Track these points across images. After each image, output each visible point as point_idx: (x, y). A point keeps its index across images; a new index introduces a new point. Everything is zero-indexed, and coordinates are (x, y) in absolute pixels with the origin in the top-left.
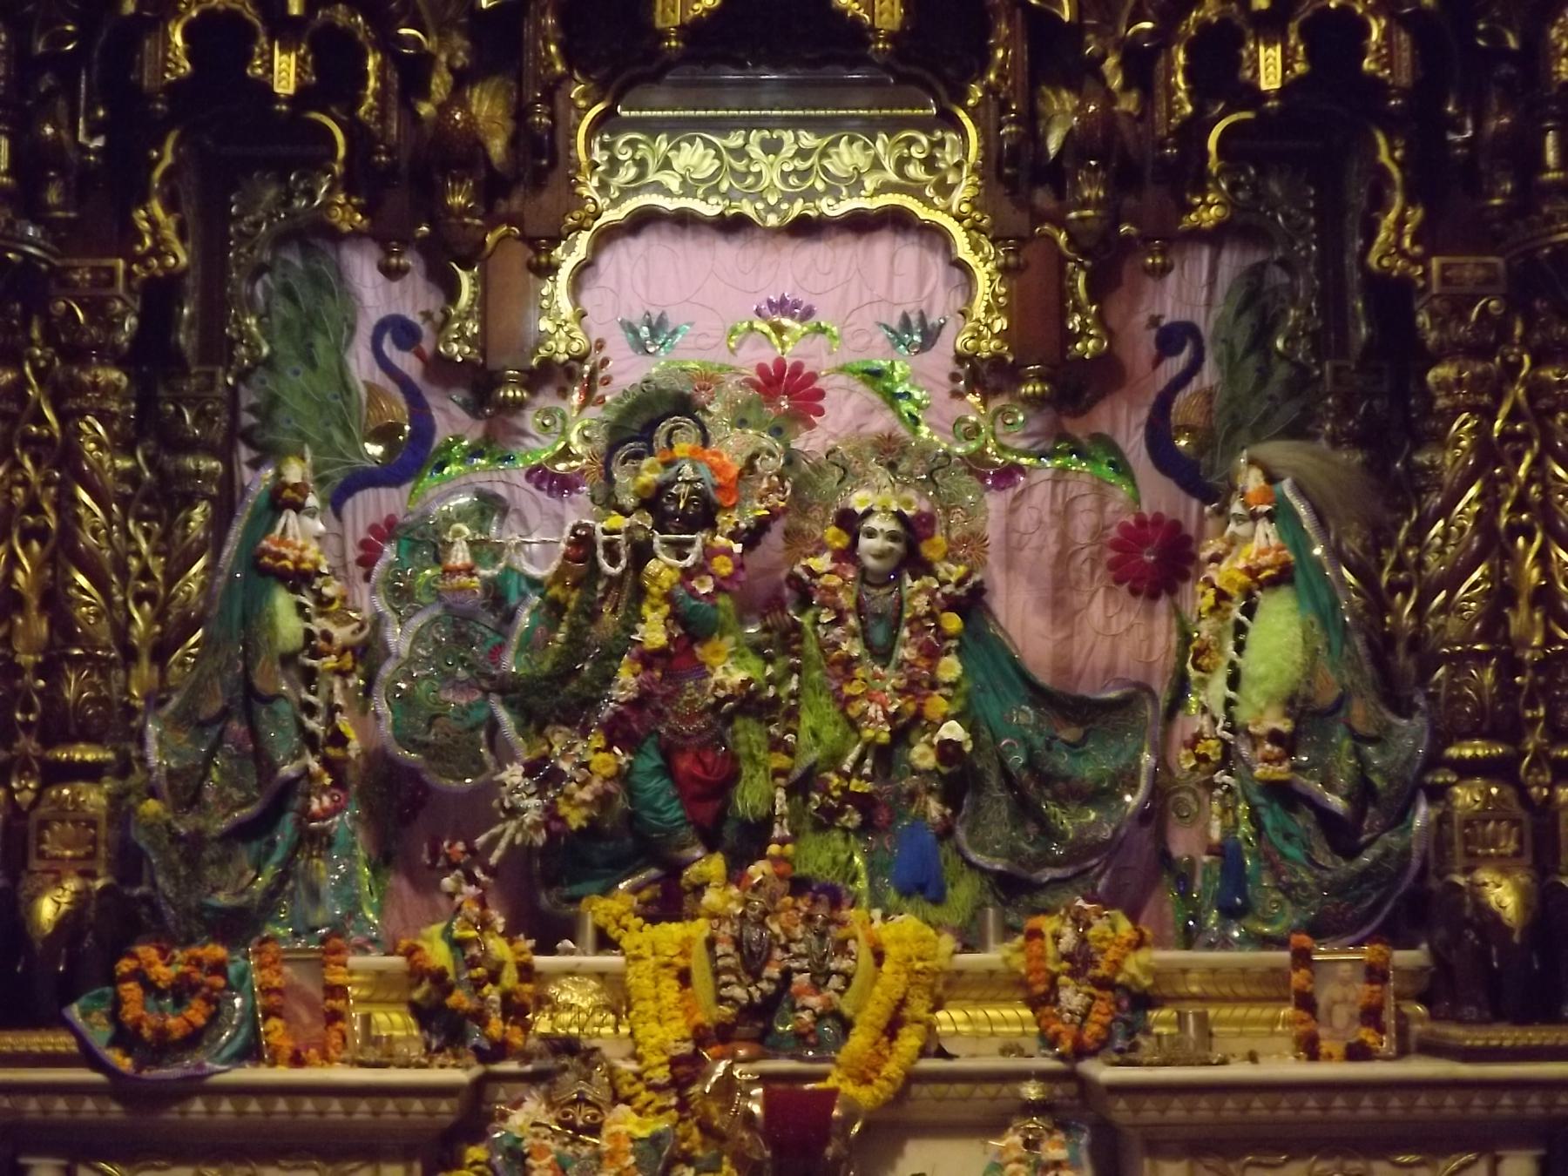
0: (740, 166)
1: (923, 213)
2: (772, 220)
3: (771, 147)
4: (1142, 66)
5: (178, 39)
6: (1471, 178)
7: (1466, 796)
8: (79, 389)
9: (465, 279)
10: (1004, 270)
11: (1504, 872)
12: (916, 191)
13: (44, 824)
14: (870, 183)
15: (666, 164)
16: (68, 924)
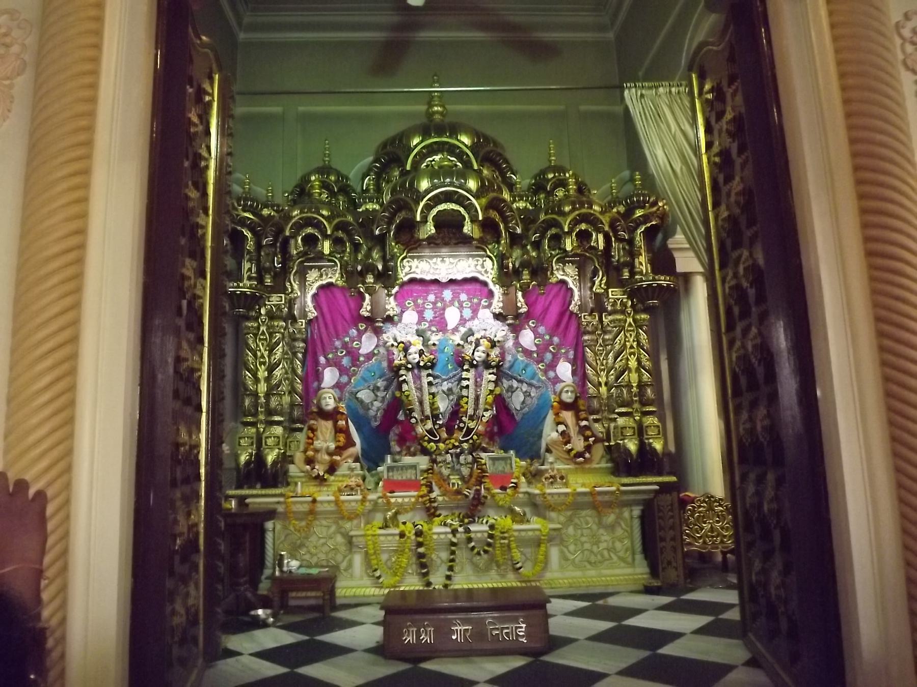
0: (436, 267)
1: (481, 278)
2: (444, 280)
3: (443, 261)
4: (537, 245)
5: (300, 241)
6: (618, 269)
7: (621, 421)
8: (273, 326)
9: (367, 296)
10: (504, 294)
11: (630, 440)
12: (480, 272)
13: (267, 438)
14: (468, 270)
15: (417, 267)
16: (275, 463)
